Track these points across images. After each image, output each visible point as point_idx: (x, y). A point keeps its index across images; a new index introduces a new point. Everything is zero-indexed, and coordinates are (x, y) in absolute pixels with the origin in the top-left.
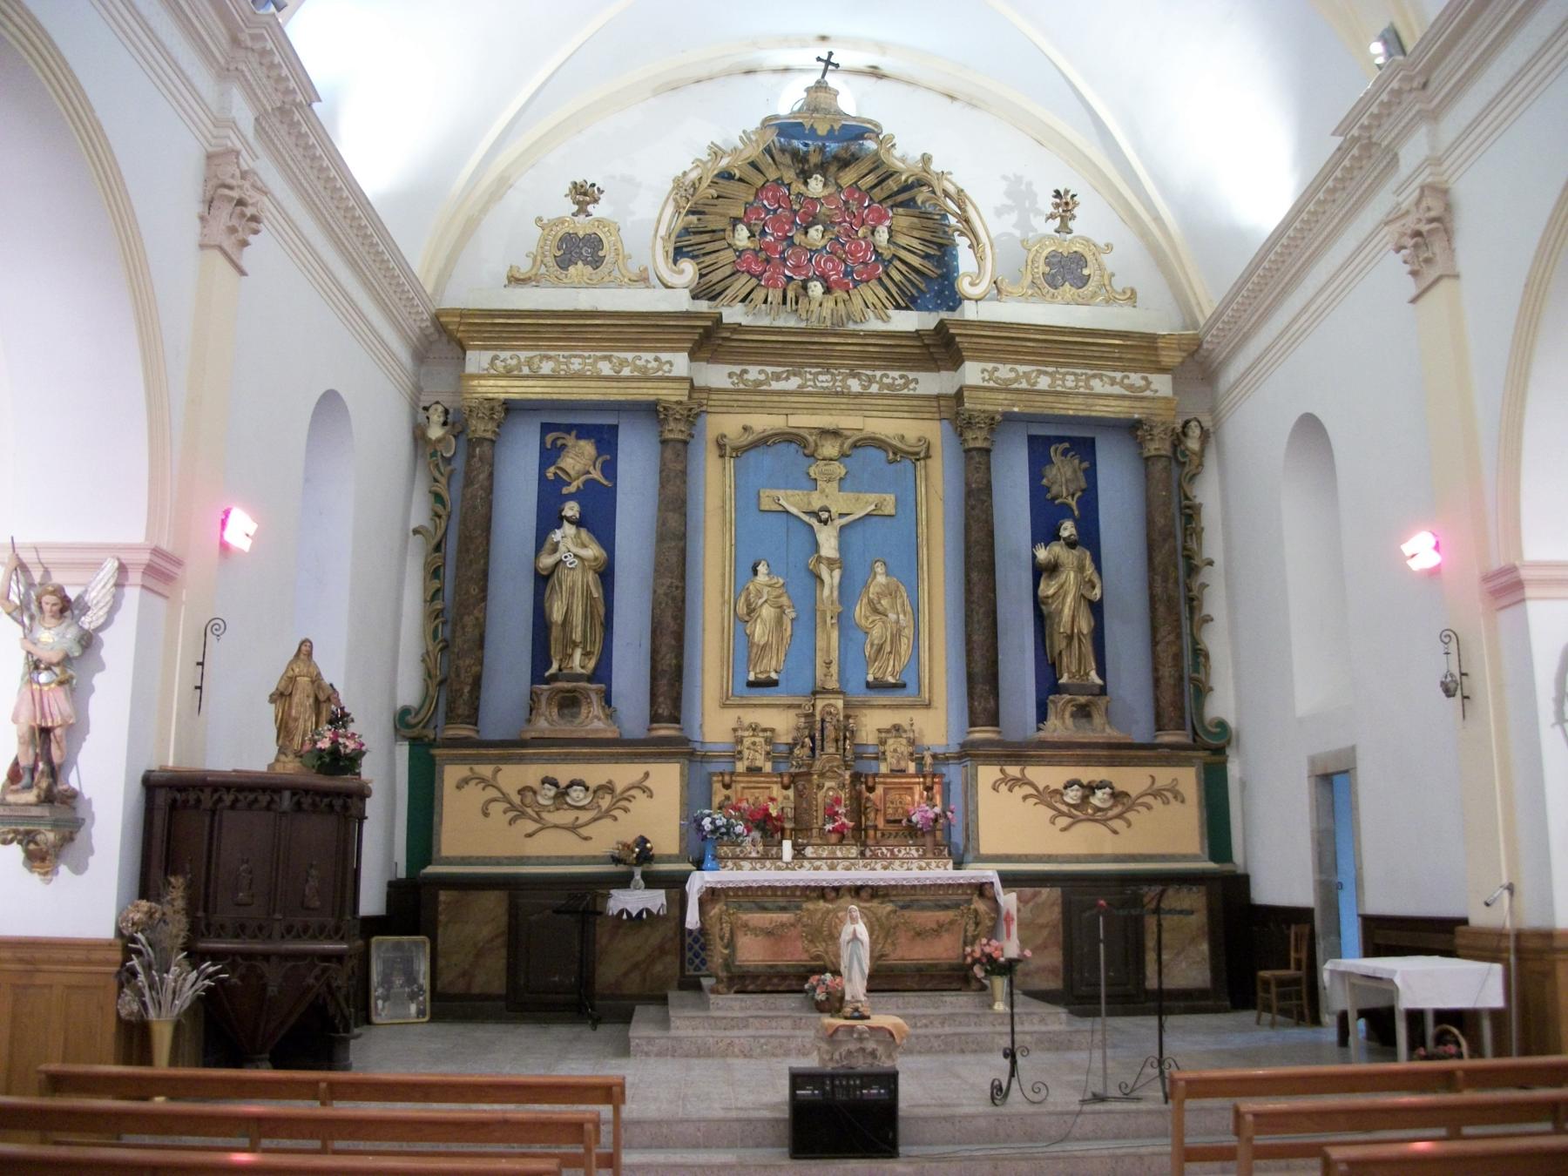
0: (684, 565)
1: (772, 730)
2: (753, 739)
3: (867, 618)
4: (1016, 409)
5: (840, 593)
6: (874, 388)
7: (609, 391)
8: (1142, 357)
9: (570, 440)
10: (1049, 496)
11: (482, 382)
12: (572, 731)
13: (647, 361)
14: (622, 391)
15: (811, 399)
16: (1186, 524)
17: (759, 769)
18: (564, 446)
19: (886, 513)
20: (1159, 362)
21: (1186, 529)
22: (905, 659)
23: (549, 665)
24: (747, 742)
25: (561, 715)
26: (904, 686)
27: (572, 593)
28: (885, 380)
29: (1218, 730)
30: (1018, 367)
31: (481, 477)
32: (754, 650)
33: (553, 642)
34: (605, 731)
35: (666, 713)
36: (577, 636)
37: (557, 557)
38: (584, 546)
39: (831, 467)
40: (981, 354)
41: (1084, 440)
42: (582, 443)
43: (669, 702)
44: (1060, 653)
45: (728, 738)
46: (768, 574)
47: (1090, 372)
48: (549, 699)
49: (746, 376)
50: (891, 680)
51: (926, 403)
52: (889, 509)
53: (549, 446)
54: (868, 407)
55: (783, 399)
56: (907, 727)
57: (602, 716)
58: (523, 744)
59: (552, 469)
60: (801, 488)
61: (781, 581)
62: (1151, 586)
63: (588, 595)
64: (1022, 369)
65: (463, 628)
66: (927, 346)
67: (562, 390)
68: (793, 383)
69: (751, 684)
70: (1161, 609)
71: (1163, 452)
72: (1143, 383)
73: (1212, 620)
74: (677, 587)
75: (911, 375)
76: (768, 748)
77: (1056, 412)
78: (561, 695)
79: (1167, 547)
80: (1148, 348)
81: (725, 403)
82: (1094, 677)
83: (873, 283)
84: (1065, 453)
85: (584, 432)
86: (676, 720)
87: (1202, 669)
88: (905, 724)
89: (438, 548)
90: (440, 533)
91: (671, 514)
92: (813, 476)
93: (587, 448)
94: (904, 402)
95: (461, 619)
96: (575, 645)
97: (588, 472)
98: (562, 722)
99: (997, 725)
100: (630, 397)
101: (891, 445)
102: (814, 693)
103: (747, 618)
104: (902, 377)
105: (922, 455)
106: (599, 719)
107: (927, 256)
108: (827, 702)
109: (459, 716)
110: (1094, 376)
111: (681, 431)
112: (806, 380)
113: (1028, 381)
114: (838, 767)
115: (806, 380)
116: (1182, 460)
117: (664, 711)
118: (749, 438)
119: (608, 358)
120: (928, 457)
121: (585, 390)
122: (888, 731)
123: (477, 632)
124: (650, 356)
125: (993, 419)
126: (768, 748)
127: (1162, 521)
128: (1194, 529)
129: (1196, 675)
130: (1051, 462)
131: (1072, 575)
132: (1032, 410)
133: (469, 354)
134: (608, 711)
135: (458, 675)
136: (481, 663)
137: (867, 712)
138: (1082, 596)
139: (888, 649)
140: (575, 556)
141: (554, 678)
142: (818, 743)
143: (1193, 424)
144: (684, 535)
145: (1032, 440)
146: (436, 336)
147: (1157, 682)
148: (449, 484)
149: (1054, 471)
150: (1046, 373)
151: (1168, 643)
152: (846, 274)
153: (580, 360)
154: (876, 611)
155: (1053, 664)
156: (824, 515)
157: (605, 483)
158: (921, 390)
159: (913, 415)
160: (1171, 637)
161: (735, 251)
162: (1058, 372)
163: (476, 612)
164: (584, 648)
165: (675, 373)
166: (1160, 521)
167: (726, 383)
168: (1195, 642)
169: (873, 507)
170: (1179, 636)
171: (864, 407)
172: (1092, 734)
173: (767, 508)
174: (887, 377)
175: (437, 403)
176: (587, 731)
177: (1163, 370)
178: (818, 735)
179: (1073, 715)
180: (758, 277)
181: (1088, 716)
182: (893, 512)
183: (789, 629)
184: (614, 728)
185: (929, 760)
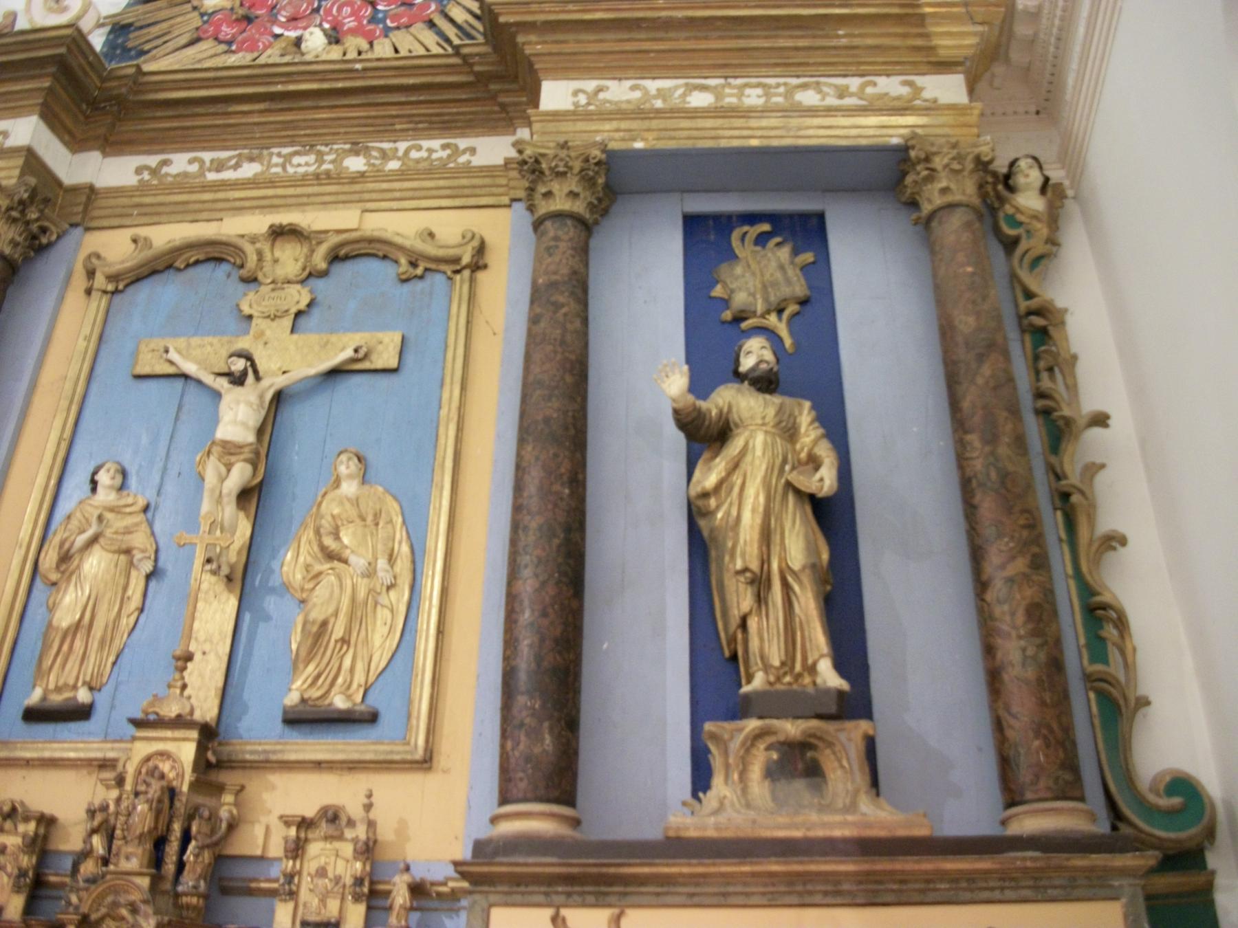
4: (639, 145)
6: (394, 165)
8: (897, 42)
10: (727, 315)
15: (270, 192)
16: (1035, 347)
19: (379, 364)
20: (932, 49)
21: (1036, 358)
26: (372, 718)
29: (1176, 801)
39: (282, 294)
40: (569, 67)
41: (804, 217)
44: (743, 624)
47: (794, 81)
49: (165, 170)
51: (487, 181)
52: (386, 357)
54: (374, 196)
55: (221, 195)
62: (961, 460)
64: (653, 85)
66: (482, 80)
68: (249, 170)
69: (34, 715)
70: (987, 506)
71: (957, 197)
72: (905, 91)
73: (1123, 541)
75: (463, 143)
77: (724, 143)
79: (986, 370)
80: (899, 19)
81: (118, 211)
82: (829, 677)
84: (762, 240)
87: (1114, 654)
88: (353, 806)
94: (442, 183)
99: (569, 799)
101: (401, 248)
104: (444, 147)
105: (466, 259)
110: (804, 86)
113: (664, 100)
115: (269, 166)
116: (1011, 232)
120: (478, 266)
122: (305, 824)
125: (587, 160)
127: (971, 320)
128: (1056, 356)
129: (1099, 667)
130: (732, 257)
131: (760, 439)
132: (671, 145)
137: (276, 778)
138: (789, 485)
143: (1023, 164)
145: (692, 224)
147: (994, 678)
149: (739, 270)
150: (704, 88)
151: (1010, 580)
152: (373, 20)
154: (330, 556)
155: (734, 657)
158: (477, 161)
159: (457, 202)
160: (1020, 565)
161: (202, 15)
162: (729, 84)
166: (966, 323)
168: (1087, 590)
169: (349, 353)
170: (1040, 563)
171: (366, 196)
172: (814, 817)
173: (146, 370)
174: (419, 148)
177: (944, 66)
179: (771, 773)
180: (229, 43)
181: (814, 772)
182: (393, 363)
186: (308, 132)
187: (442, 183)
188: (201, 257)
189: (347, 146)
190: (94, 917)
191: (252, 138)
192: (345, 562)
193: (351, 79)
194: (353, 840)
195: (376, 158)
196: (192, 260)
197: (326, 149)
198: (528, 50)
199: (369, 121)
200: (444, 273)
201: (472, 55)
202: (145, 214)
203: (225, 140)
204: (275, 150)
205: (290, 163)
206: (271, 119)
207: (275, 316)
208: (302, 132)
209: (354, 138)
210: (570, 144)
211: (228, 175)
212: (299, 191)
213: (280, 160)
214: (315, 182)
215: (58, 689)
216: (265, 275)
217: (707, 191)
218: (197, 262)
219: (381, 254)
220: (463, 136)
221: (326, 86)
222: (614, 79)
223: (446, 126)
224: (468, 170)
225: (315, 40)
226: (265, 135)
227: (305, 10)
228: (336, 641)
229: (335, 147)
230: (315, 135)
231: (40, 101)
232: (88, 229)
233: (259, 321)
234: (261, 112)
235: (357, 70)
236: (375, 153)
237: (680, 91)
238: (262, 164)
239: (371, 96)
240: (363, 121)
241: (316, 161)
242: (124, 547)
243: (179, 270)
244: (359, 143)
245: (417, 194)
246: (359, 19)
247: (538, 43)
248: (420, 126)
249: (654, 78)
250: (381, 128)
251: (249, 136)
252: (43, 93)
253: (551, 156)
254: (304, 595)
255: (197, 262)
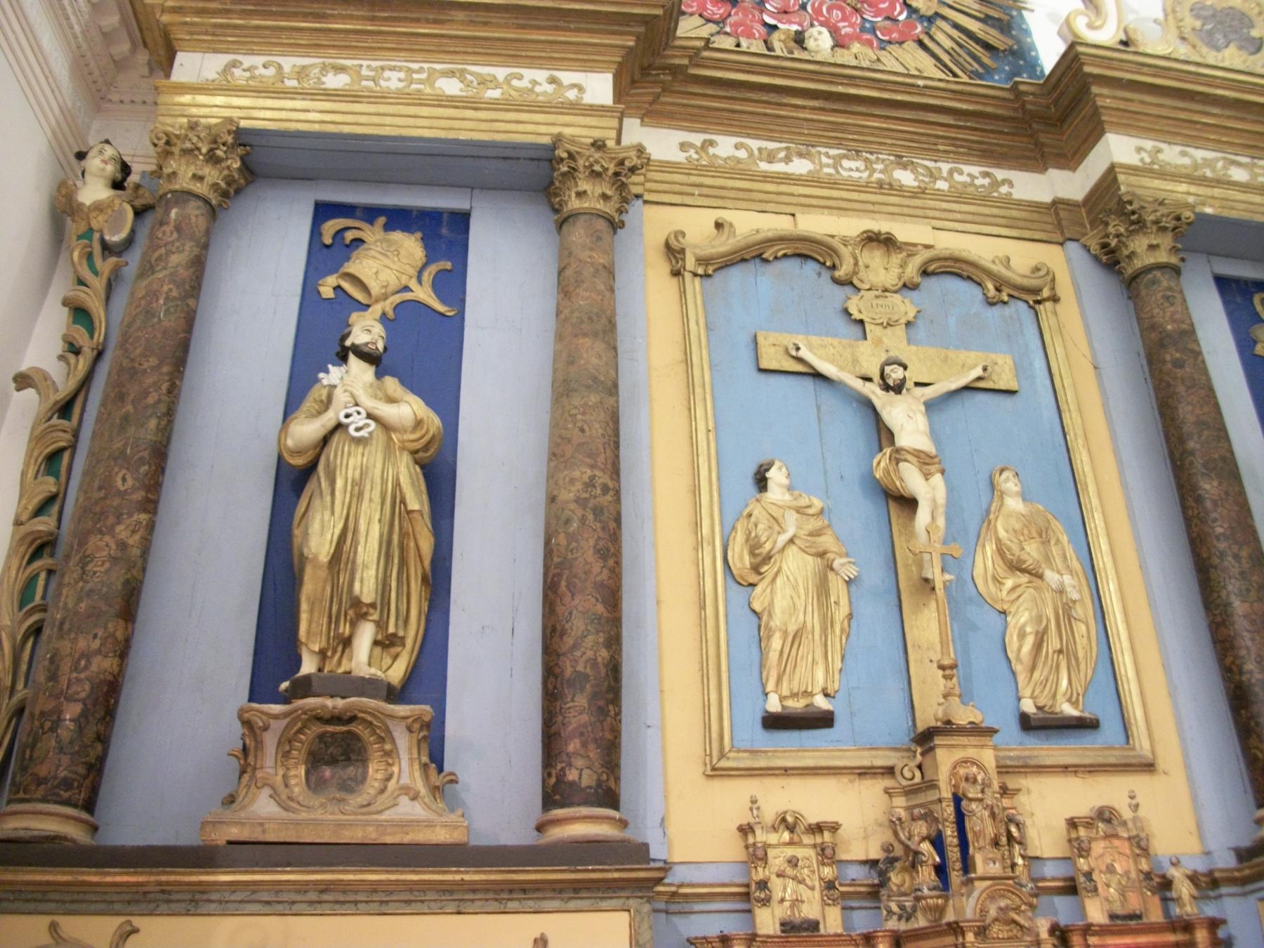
0: (617, 445)
1: (834, 828)
2: (790, 852)
3: (998, 581)
4: (1209, 210)
5: (949, 520)
6: (942, 185)
7: (457, 124)
9: (373, 234)
11: (202, 99)
12: (340, 825)
13: (535, 83)
14: (484, 126)
15: (835, 193)
17: (813, 926)
18: (359, 242)
22: (1086, 669)
23: (298, 662)
24: (777, 859)
25: (315, 784)
27: (358, 494)
28: (957, 177)
30: (1191, 151)
31: (175, 259)
32: (776, 643)
33: (304, 606)
34: (430, 825)
35: (588, 779)
36: (366, 586)
37: (328, 419)
38: (391, 400)
40: (1132, 124)
42: (397, 236)
43: (594, 753)
45: (733, 850)
46: (790, 489)
48: (286, 742)
49: (711, 151)
50: (1069, 710)
53: (328, 240)
54: (937, 214)
56: (1127, 814)
57: (420, 786)
58: (203, 857)
59: (332, 280)
60: (835, 335)
61: (818, 504)
63: (398, 500)
64: (1200, 154)
65: (84, 563)
67: (363, 119)
68: (800, 167)
69: (774, 722)
74: (605, 489)
75: (1000, 174)
76: (828, 872)
78: (317, 729)
81: (677, 188)
83: (910, 45)
85: (399, 219)
86: (609, 798)
89: (65, 409)
90: (72, 384)
91: (587, 342)
92: (857, 316)
93: (410, 246)
94: (995, 211)
95: (82, 543)
96: (359, 611)
97: (406, 289)
98: (316, 801)
100: (499, 137)
102: (926, 739)
103: (753, 578)
104: (986, 175)
106: (414, 798)
107: (986, 20)
108: (959, 754)
109: (40, 781)
111: (605, 197)
112: (822, 165)
114: (1017, 909)
117: (581, 773)
118: (723, 245)
119: (461, 75)
121: (411, 121)
122: (1089, 824)
123: (117, 579)
124: (541, 75)
125: (1178, 218)
126: (828, 872)
133: (181, 57)
134: (436, 779)
135: (53, 677)
136: (123, 651)
139: (1053, 643)
140: (370, 416)
141: (304, 687)
142: (954, 853)
144: (616, 385)
146: (123, 47)
148: (110, 288)
152: (863, 29)
153: (402, 75)
154: (1016, 567)
156: (895, 374)
157: (440, 308)
158: (1018, 194)
163: (122, 531)
164: (381, 625)
165: (588, 99)
167: (680, 157)
169: (978, 372)
173: (774, 365)
174: (961, 173)
175: (107, 142)
176: (380, 825)
178: (950, 833)
180: (721, 22)
182: (1013, 385)
183: (844, 601)
184: (453, 818)
185: (1184, 889)
186: (856, 137)
187: (995, 211)
188: (789, 252)
189: (892, 158)
190: (988, 921)
191: (799, 134)
192: (1040, 577)
193: (909, 93)
194: (1129, 839)
195: (923, 175)
196: (780, 254)
197: (873, 157)
198: (1100, 102)
199: (916, 137)
200: (1026, 302)
201: (1026, 93)
202: (707, 196)
203: (772, 130)
204: (823, 150)
205: (841, 166)
206: (823, 118)
207: (888, 324)
208: (850, 137)
209: (898, 151)
210: (1166, 202)
211: (779, 167)
212: (863, 197)
213: (830, 161)
214: (877, 191)
215: (794, 695)
216: (862, 281)
217: (1227, 256)
218: (785, 256)
219: (965, 274)
220: (998, 166)
221: (886, 95)
222: (1165, 142)
223: (990, 155)
224: (1008, 202)
225: (820, 41)
226: (813, 132)
227: (794, 5)
228: (1054, 652)
229: (880, 156)
230: (863, 141)
231: (619, 59)
232: (646, 202)
233: (872, 327)
234: (813, 109)
235: (919, 86)
236: (920, 170)
237: (1220, 164)
238: (813, 163)
239: (922, 113)
240: (908, 136)
241: (867, 168)
242: (821, 550)
243: (766, 261)
244: (903, 157)
245: (976, 218)
246: (852, 25)
247: (1108, 97)
248: (961, 150)
249: (1197, 148)
250: (925, 146)
251: (796, 130)
252: (623, 52)
253: (1150, 210)
254: (1005, 607)
255: (785, 256)
